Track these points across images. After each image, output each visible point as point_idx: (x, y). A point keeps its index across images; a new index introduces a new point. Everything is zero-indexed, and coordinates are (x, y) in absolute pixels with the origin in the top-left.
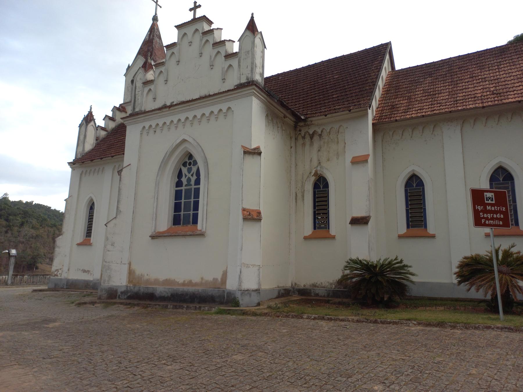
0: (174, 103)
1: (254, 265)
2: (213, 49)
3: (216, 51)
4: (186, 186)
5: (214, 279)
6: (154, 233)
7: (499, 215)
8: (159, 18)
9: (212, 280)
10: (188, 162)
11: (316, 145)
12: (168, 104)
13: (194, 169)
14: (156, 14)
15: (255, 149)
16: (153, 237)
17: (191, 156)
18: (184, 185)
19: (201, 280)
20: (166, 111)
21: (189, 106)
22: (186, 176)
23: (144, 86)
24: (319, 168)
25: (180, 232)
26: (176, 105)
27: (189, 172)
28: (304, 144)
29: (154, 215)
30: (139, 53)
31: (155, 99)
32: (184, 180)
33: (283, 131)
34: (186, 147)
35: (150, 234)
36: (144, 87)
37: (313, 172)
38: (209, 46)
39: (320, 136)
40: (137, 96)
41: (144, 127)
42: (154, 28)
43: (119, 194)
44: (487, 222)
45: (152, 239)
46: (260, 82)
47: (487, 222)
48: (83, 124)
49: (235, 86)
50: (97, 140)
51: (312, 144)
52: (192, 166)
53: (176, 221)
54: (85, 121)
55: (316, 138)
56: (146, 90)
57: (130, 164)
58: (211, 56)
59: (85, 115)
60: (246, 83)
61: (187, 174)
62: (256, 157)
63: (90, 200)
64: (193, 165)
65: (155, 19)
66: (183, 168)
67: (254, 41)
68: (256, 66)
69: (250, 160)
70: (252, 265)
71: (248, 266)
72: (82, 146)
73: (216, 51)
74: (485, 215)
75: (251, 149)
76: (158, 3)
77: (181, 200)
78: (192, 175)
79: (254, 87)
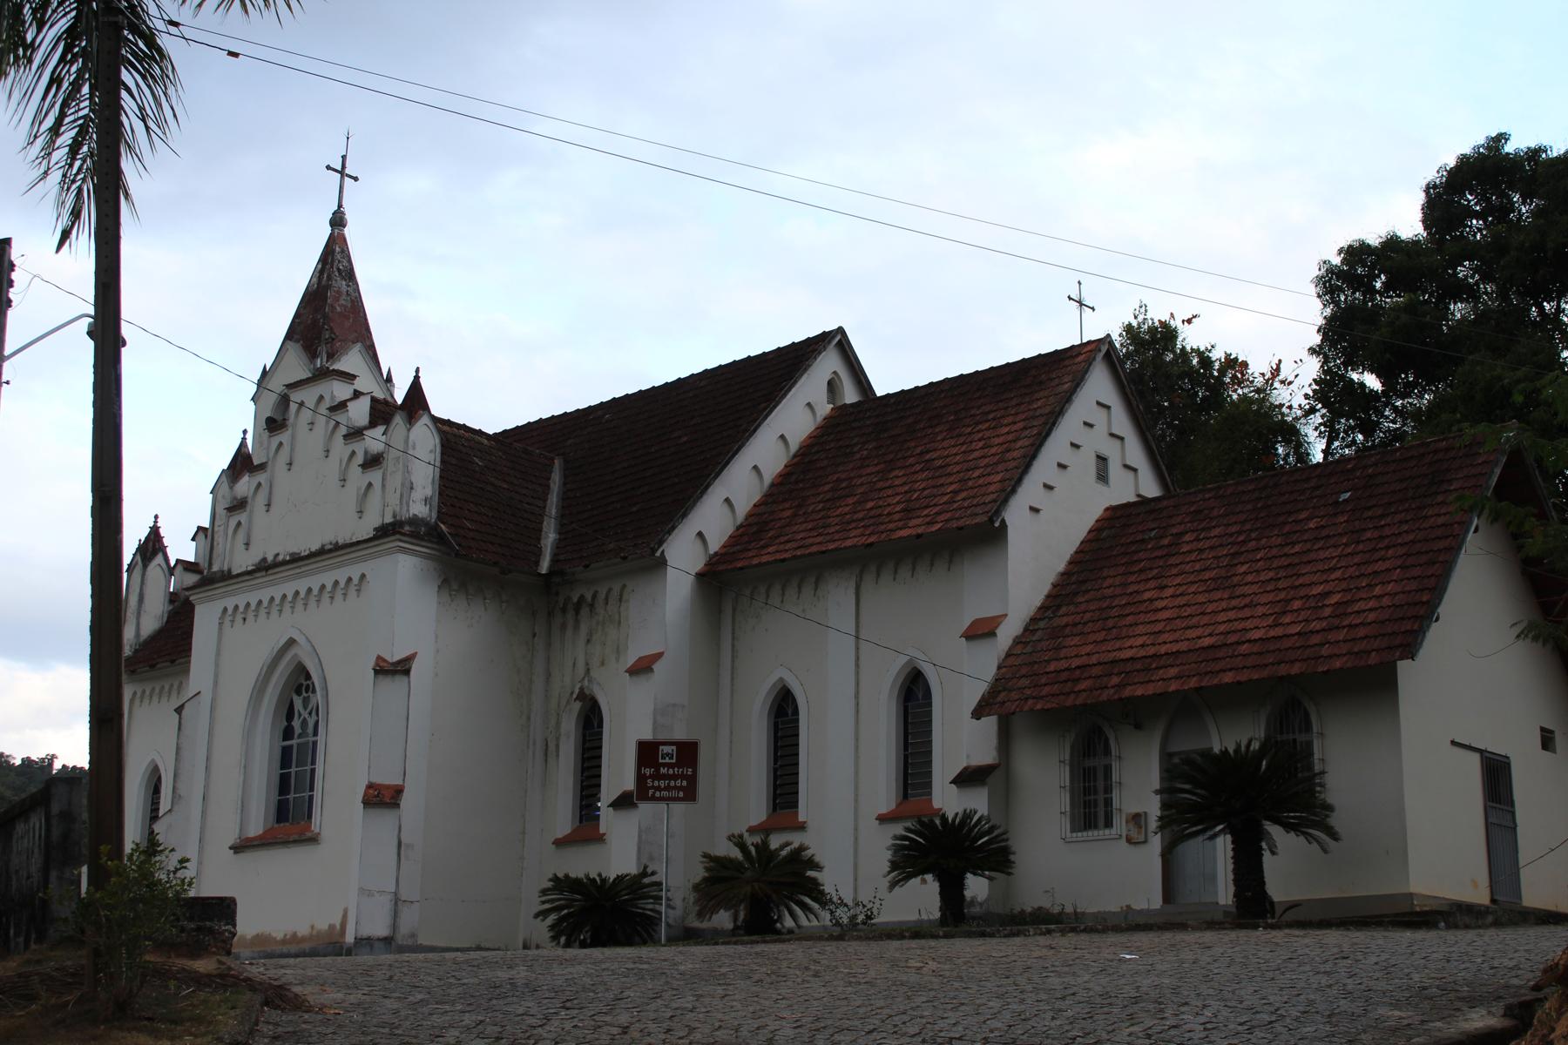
0: (281, 558)
1: (381, 892)
2: (345, 444)
3: (350, 448)
4: (300, 736)
5: (330, 925)
6: (238, 841)
7: (679, 781)
8: (348, 216)
9: (327, 928)
10: (305, 683)
12: (270, 558)
13: (312, 704)
14: (340, 206)
15: (400, 662)
16: (238, 848)
17: (302, 672)
18: (296, 736)
19: (310, 930)
20: (261, 579)
21: (299, 567)
22: (300, 715)
23: (229, 514)
24: (586, 683)
25: (281, 836)
26: (284, 563)
27: (305, 708)
28: (563, 627)
29: (240, 802)
31: (247, 544)
32: (296, 723)
33: (504, 605)
34: (296, 655)
36: (229, 517)
37: (577, 691)
39: (592, 606)
40: (216, 538)
41: (225, 610)
42: (334, 251)
43: (176, 760)
44: (657, 794)
45: (235, 853)
46: (425, 516)
47: (657, 794)
48: (137, 563)
49: (375, 529)
50: (171, 601)
51: (577, 627)
52: (310, 694)
53: (282, 812)
54: (141, 555)
55: (585, 611)
57: (199, 693)
58: (341, 461)
59: (140, 540)
60: (390, 524)
61: (302, 711)
62: (400, 680)
63: (150, 770)
64: (312, 693)
65: (338, 221)
66: (295, 697)
67: (408, 437)
68: (412, 488)
69: (394, 685)
70: (378, 892)
71: (370, 894)
73: (350, 448)
74: (656, 783)
75: (393, 664)
76: (347, 171)
77: (290, 768)
78: (310, 714)
79: (398, 536)
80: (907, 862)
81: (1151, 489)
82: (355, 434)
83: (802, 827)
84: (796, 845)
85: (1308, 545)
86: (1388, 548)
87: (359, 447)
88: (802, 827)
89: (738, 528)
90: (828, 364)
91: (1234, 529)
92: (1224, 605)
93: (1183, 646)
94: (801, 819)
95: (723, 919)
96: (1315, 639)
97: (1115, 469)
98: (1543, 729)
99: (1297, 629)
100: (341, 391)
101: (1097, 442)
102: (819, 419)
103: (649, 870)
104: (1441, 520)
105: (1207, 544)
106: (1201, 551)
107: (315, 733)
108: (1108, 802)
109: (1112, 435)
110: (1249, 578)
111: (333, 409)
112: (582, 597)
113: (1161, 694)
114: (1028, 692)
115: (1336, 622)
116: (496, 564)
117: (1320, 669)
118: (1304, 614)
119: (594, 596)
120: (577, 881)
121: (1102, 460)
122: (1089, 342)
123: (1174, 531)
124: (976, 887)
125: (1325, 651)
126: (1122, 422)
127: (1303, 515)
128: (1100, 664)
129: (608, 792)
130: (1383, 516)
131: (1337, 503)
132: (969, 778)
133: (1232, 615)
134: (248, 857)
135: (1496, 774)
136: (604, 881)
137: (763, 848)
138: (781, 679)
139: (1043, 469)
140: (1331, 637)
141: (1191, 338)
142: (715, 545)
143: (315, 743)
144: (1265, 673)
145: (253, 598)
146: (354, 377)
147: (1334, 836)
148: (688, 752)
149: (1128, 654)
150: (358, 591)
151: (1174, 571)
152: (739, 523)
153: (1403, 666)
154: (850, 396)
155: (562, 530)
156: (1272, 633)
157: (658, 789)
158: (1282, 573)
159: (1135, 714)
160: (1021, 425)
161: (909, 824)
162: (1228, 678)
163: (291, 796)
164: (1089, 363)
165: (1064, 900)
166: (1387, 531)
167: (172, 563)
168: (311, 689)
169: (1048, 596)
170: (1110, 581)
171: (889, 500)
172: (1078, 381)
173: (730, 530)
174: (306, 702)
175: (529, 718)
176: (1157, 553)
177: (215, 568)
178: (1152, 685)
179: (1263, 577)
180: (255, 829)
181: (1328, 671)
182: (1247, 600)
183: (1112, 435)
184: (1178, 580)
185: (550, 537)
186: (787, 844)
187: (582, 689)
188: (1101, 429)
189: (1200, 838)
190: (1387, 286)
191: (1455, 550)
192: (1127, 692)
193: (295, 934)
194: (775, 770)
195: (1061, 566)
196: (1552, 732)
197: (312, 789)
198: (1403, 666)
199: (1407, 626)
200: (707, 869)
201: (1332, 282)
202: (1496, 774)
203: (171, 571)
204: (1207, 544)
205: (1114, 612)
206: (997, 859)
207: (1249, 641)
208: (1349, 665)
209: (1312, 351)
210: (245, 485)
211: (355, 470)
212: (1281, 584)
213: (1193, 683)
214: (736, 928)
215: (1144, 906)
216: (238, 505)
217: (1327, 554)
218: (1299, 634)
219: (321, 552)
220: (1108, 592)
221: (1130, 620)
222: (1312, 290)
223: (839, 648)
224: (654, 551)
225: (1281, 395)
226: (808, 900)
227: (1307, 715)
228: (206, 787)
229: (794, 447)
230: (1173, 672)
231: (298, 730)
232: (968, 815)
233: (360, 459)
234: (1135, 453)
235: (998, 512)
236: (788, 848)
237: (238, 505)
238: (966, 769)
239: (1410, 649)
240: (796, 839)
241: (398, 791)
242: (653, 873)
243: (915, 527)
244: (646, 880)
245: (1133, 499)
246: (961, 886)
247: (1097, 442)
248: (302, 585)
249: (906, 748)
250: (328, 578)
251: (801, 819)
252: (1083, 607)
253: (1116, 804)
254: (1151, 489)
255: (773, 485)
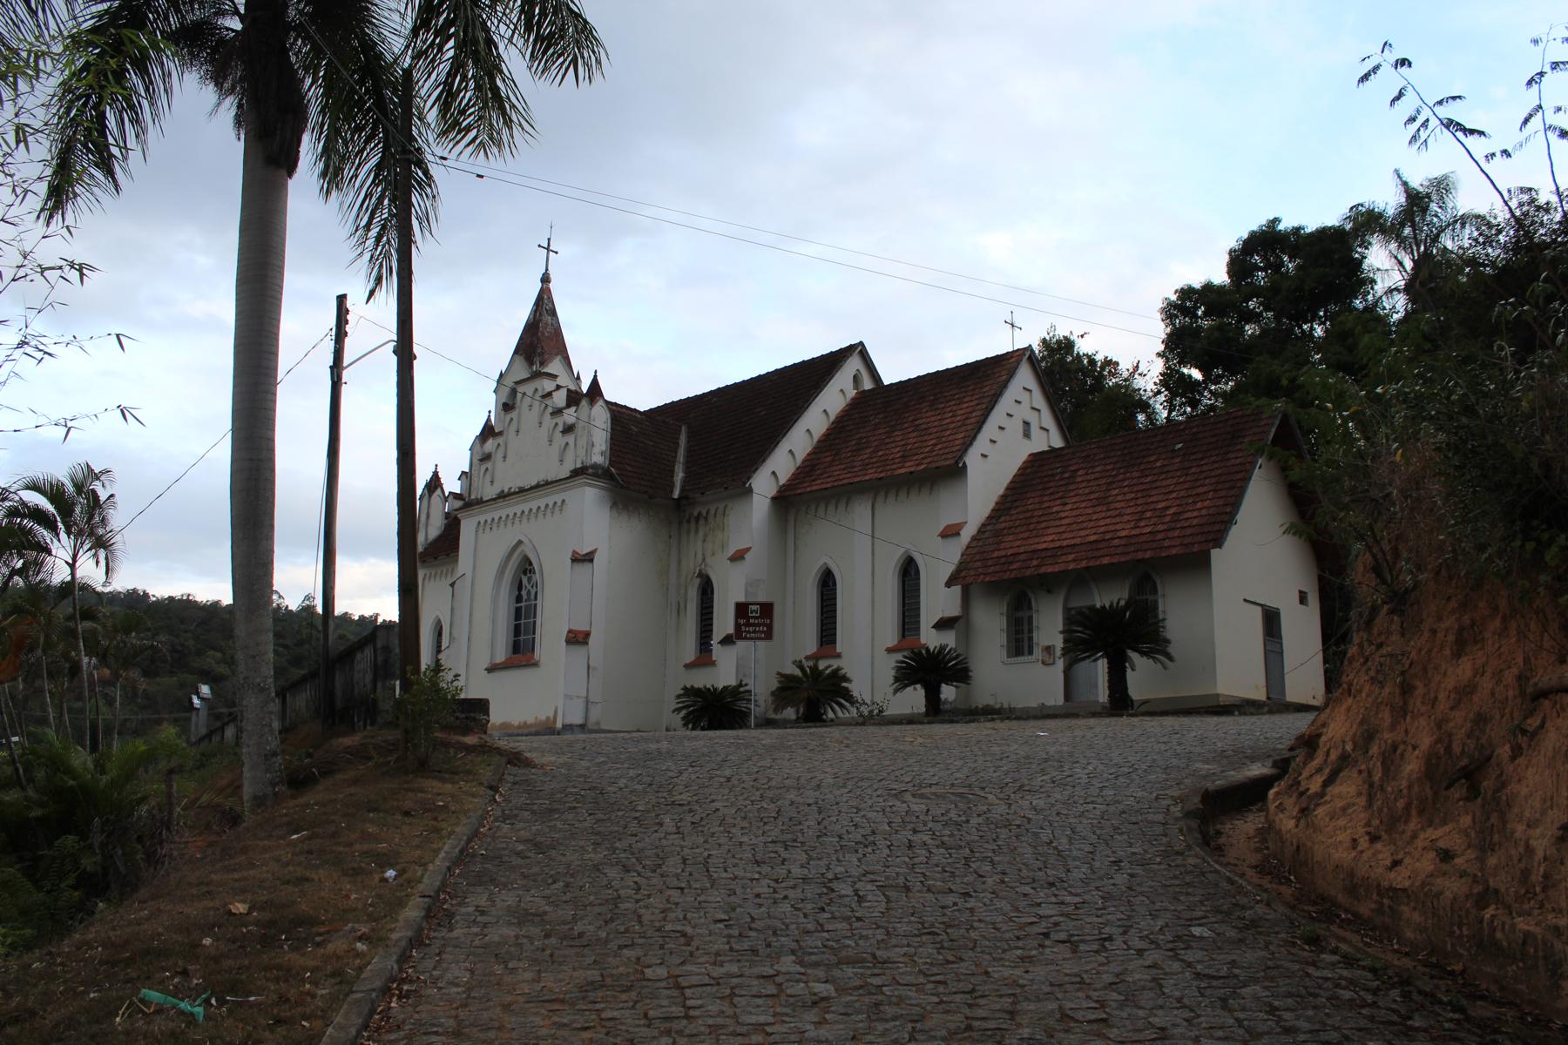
1: (578, 697)
3: (554, 421)
11: (701, 533)
12: (506, 491)
13: (533, 581)
14: (547, 270)
15: (587, 554)
20: (501, 503)
26: (515, 493)
27: (529, 583)
28: (688, 532)
30: (516, 352)
31: (492, 482)
32: (524, 593)
35: (486, 666)
38: (547, 415)
39: (706, 519)
41: (479, 522)
50: (446, 518)
51: (697, 531)
53: (516, 648)
55: (702, 522)
56: (483, 468)
62: (587, 566)
65: (546, 279)
68: (593, 446)
72: (424, 534)
73: (554, 421)
80: (905, 678)
81: (1058, 442)
82: (558, 412)
83: (839, 656)
84: (835, 667)
85: (1156, 477)
86: (1205, 478)
87: (560, 420)
88: (839, 656)
89: (797, 469)
90: (853, 364)
91: (1108, 467)
92: (1103, 515)
93: (1078, 541)
94: (838, 651)
95: (790, 713)
96: (1160, 536)
97: (1035, 430)
98: (1300, 592)
99: (1148, 530)
100: (548, 385)
101: (1024, 413)
102: (848, 399)
103: (744, 683)
104: (1238, 461)
105: (1093, 476)
106: (1089, 481)
107: (536, 599)
108: (1030, 639)
109: (1033, 408)
110: (1119, 498)
111: (544, 397)
112: (700, 514)
113: (1064, 571)
114: (980, 570)
115: (1173, 525)
116: (646, 492)
117: (1164, 555)
118: (1153, 521)
119: (708, 512)
120: (699, 690)
121: (1026, 424)
122: (1018, 350)
123: (1072, 468)
124: (948, 692)
125: (1166, 543)
126: (1039, 400)
127: (1152, 459)
128: (1025, 552)
129: (717, 635)
130: (1202, 459)
131: (1174, 451)
132: (943, 624)
133: (1108, 521)
134: (497, 675)
135: (1271, 620)
136: (715, 689)
137: (814, 669)
138: (825, 564)
139: (989, 430)
140: (1170, 534)
141: (1083, 347)
142: (783, 480)
143: (536, 605)
144: (1128, 558)
145: (496, 515)
146: (556, 376)
147: (1171, 659)
148: (767, 609)
149: (1044, 546)
150: (561, 510)
151: (1072, 494)
152: (798, 465)
153: (1215, 553)
154: (868, 385)
155: (687, 470)
156: (1133, 532)
157: (749, 632)
158: (1139, 495)
159: (1047, 584)
160: (976, 402)
161: (906, 654)
162: (1105, 561)
163: (522, 638)
164: (1018, 363)
165: (1004, 701)
166: (1205, 468)
167: (447, 494)
168: (532, 571)
169: (993, 510)
170: (1031, 501)
171: (893, 450)
172: (1011, 374)
173: (792, 470)
174: (529, 580)
175: (667, 589)
176: (1063, 483)
177: (473, 497)
178: (1057, 566)
179: (1129, 496)
180: (501, 657)
181: (1168, 556)
182: (1118, 512)
183: (1033, 408)
184: (1074, 500)
185: (679, 476)
186: (830, 666)
187: (700, 571)
188: (1026, 405)
189: (1088, 661)
190: (1205, 314)
191: (1246, 479)
192: (1043, 570)
193: (525, 722)
194: (822, 620)
195: (1001, 491)
196: (1305, 593)
197: (534, 633)
198: (1215, 553)
199: (1217, 527)
200: (780, 682)
201: (1172, 311)
202: (1271, 620)
203: (446, 499)
204: (1093, 476)
205: (1034, 520)
206: (961, 675)
207: (1119, 538)
208: (1181, 552)
209: (1159, 355)
210: (490, 445)
211: (558, 434)
212: (1139, 502)
213: (1084, 564)
214: (798, 718)
215: (1053, 704)
216: (486, 458)
217: (1168, 482)
218: (1150, 533)
219: (538, 486)
220: (1030, 507)
221: (1043, 525)
222: (1159, 316)
223: (862, 543)
224: (745, 483)
225: (1139, 383)
226: (843, 701)
227: (1155, 583)
228: (470, 632)
229: (832, 418)
230: (1071, 557)
231: (525, 597)
232: (943, 648)
233: (560, 428)
234: (1048, 420)
235: (961, 457)
236: (830, 669)
237: (486, 458)
238: (941, 619)
239: (1218, 542)
240: (835, 663)
241: (587, 634)
242: (746, 685)
243: (909, 467)
244: (742, 689)
245: (1047, 449)
246: (938, 692)
247: (1024, 413)
248: (526, 507)
249: (904, 606)
250: (542, 503)
251: (838, 651)
252: (1014, 518)
253: (1035, 640)
254: (1058, 442)
255: (819, 441)
